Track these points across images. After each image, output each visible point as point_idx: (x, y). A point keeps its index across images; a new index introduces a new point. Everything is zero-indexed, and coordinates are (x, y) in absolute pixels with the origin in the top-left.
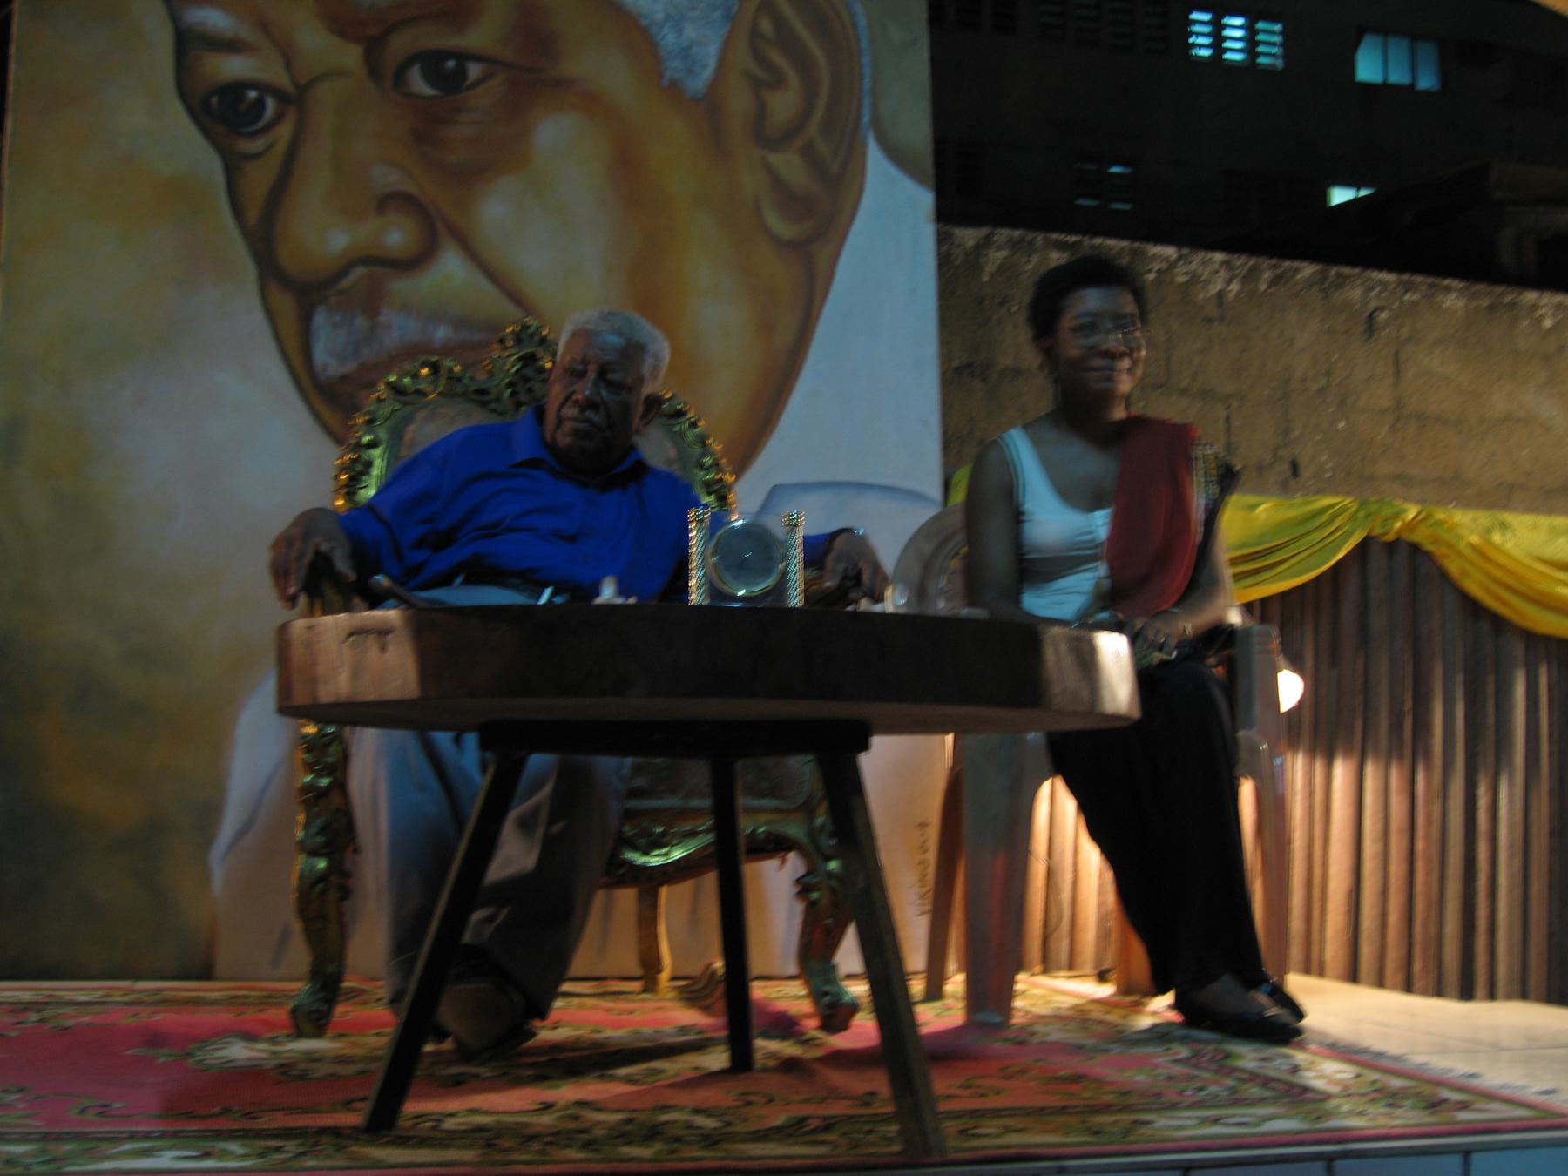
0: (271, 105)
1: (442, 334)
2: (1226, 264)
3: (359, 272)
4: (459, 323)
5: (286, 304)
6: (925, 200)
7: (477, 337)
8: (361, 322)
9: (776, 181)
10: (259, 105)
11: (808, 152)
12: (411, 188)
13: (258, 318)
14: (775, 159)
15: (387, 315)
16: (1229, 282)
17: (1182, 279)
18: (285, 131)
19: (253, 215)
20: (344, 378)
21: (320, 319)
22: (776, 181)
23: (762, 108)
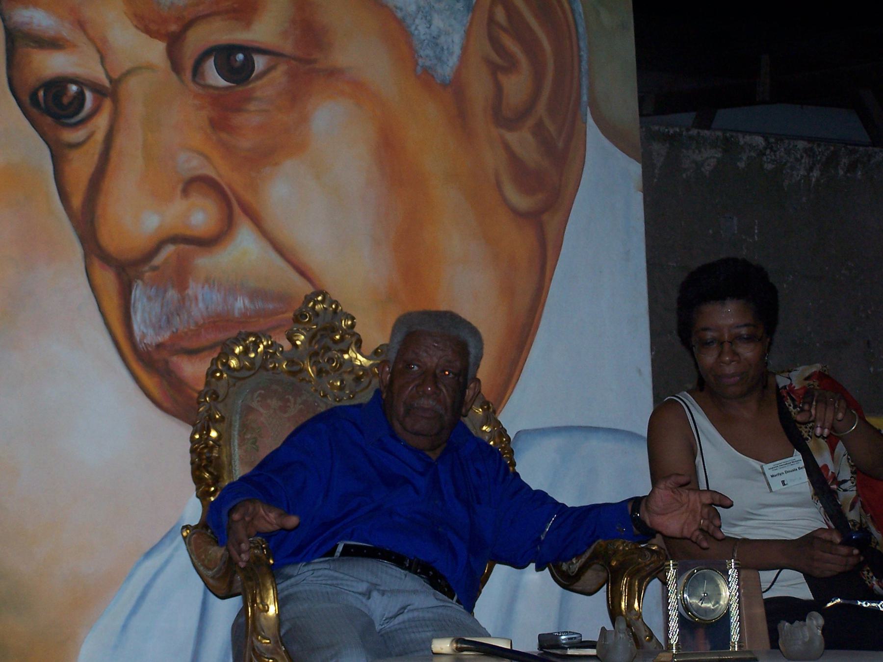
0: (89, 95)
1: (240, 304)
2: (809, 152)
3: (169, 250)
4: (254, 294)
5: (107, 279)
6: (635, 169)
7: (271, 306)
8: (172, 294)
9: (514, 159)
10: (80, 96)
11: (539, 130)
12: (212, 173)
13: (86, 290)
14: (512, 137)
15: (194, 288)
16: (811, 169)
17: (769, 167)
18: (102, 122)
19: (77, 201)
20: (159, 346)
21: (138, 293)
22: (514, 159)
23: (499, 89)
